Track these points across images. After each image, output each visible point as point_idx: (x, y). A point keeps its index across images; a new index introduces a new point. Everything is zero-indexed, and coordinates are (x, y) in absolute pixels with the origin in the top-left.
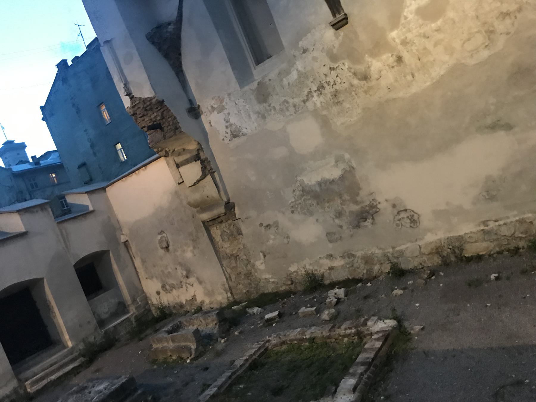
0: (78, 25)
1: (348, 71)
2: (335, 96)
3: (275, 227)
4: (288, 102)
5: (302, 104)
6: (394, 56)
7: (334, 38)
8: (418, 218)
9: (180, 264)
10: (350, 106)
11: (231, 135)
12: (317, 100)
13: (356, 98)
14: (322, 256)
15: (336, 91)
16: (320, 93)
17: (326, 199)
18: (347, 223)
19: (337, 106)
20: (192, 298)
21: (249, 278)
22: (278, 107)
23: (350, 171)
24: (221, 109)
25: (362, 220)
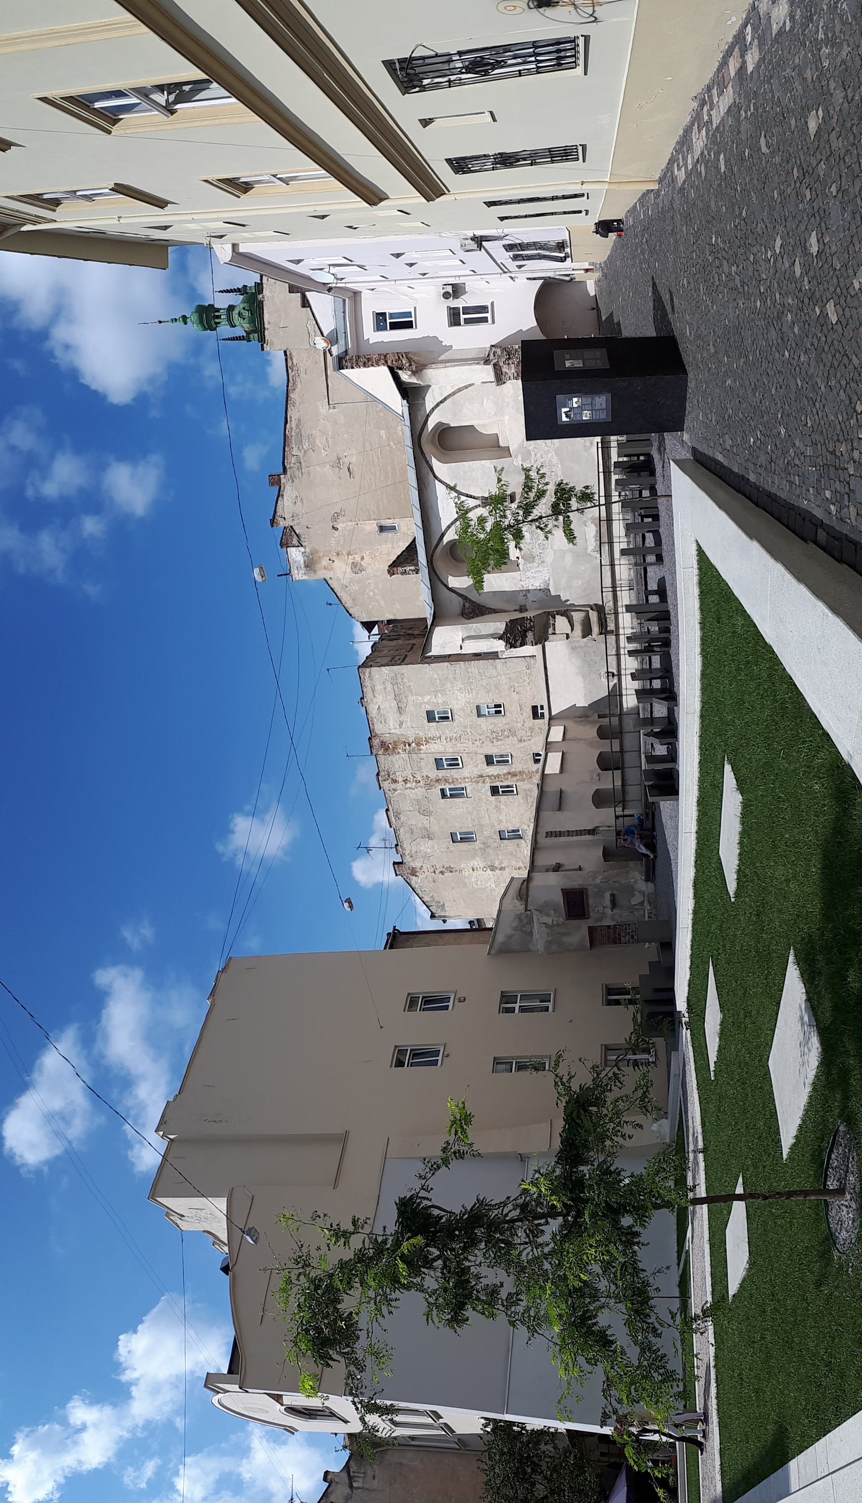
22: (541, 551)
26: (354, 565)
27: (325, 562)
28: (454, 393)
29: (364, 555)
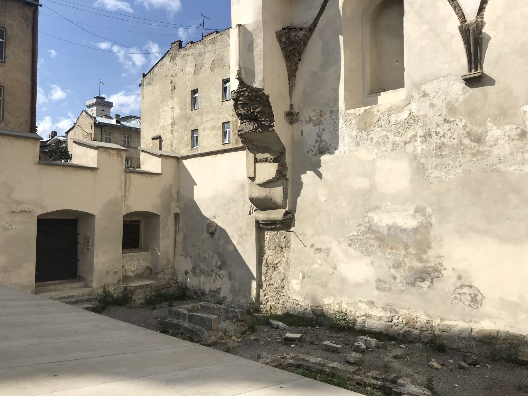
0: (204, 16)
1: (463, 129)
2: (440, 148)
3: (325, 253)
4: (388, 138)
5: (403, 144)
6: (519, 130)
7: (460, 92)
8: (481, 300)
9: (219, 254)
10: (452, 163)
11: (317, 150)
12: (419, 146)
13: (461, 157)
14: (363, 300)
15: (443, 143)
16: (425, 141)
17: (390, 245)
18: (403, 276)
19: (438, 158)
20: (217, 291)
21: (280, 293)
22: (375, 140)
23: (426, 227)
24: (318, 123)
25: (420, 279)
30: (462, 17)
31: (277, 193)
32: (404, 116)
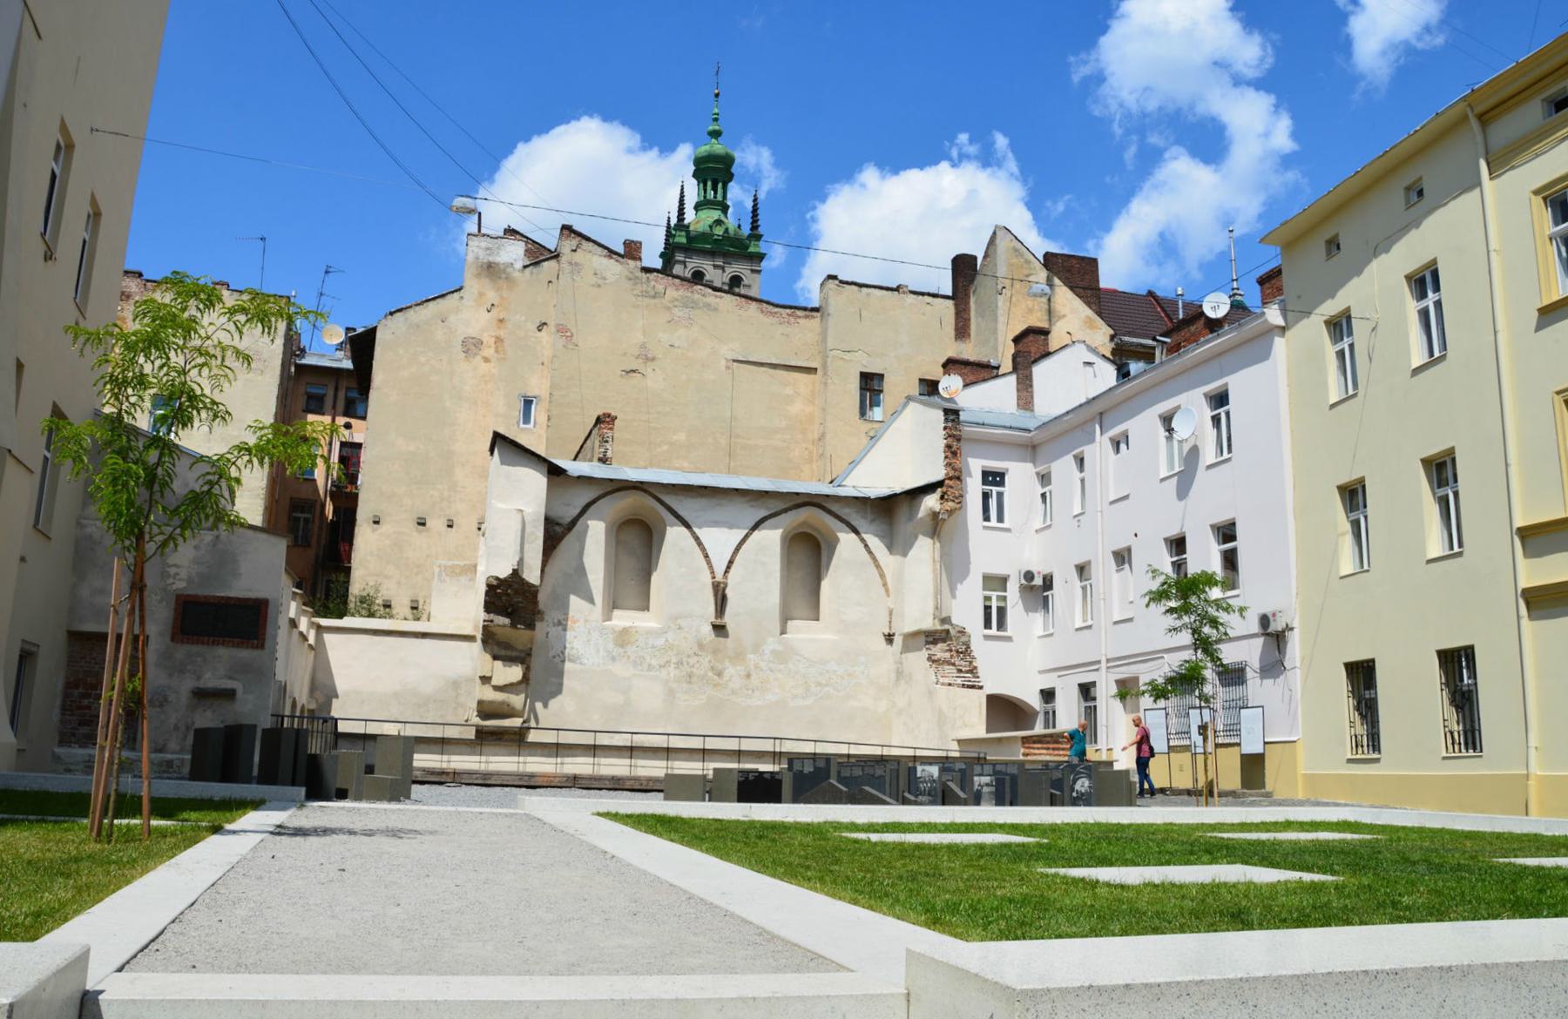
12: (673, 672)
26: (479, 343)
27: (492, 296)
28: (878, 566)
29: (492, 364)
30: (713, 572)
31: (517, 700)
32: (661, 642)
